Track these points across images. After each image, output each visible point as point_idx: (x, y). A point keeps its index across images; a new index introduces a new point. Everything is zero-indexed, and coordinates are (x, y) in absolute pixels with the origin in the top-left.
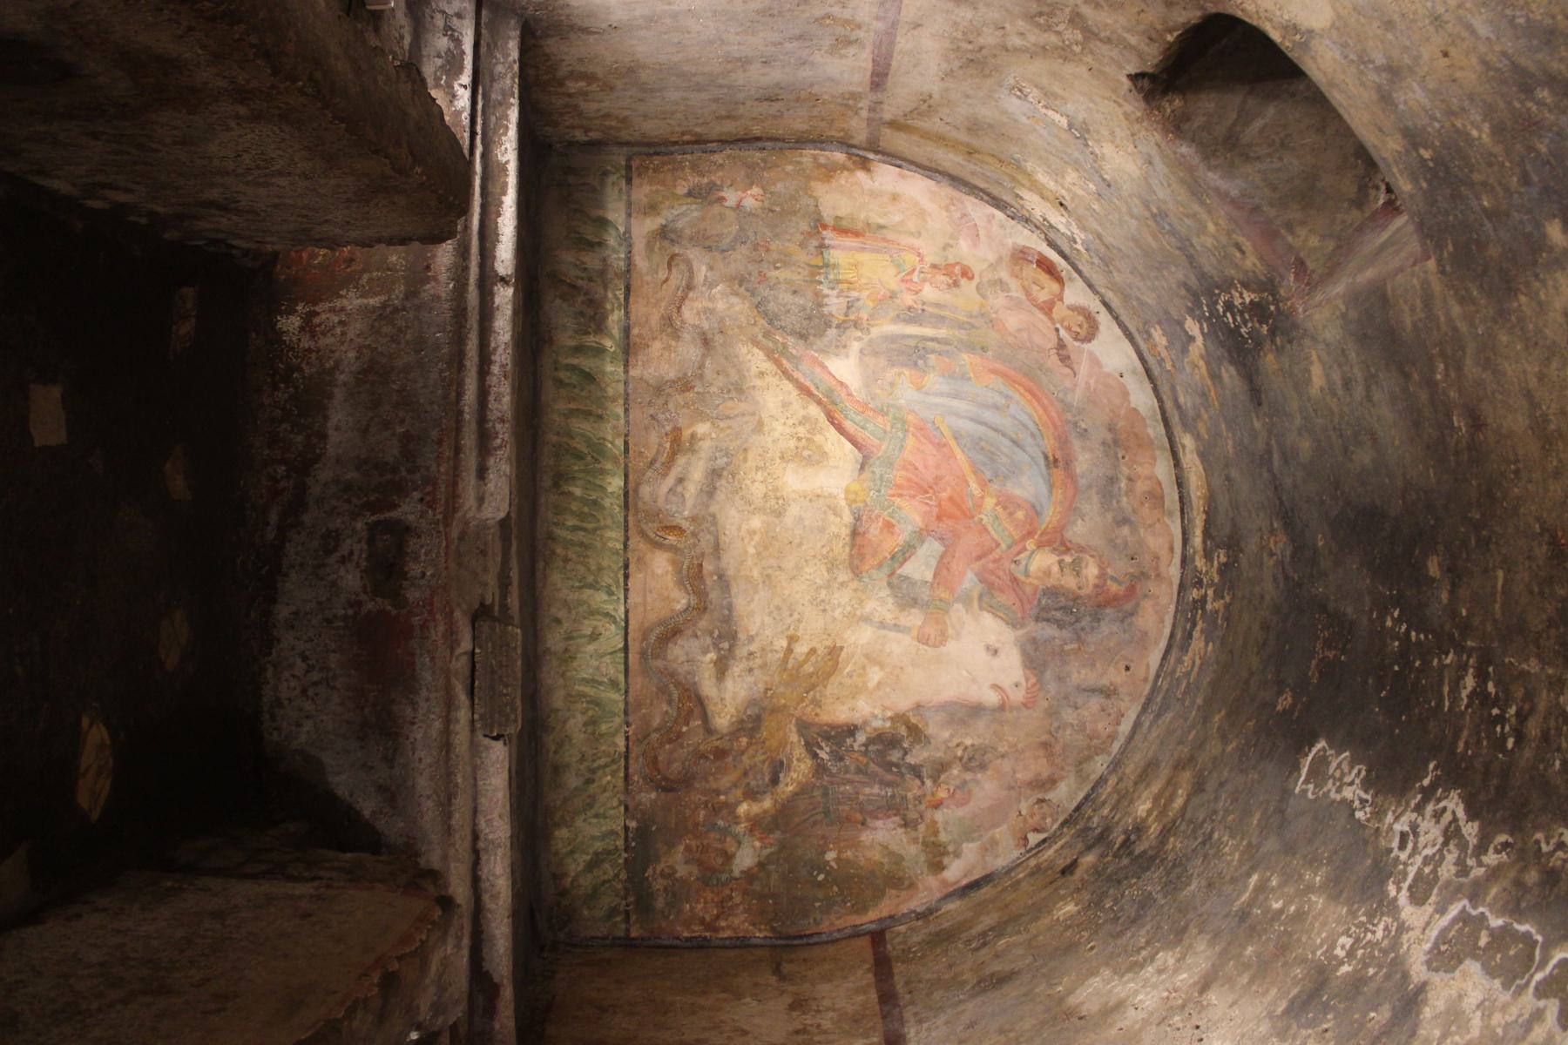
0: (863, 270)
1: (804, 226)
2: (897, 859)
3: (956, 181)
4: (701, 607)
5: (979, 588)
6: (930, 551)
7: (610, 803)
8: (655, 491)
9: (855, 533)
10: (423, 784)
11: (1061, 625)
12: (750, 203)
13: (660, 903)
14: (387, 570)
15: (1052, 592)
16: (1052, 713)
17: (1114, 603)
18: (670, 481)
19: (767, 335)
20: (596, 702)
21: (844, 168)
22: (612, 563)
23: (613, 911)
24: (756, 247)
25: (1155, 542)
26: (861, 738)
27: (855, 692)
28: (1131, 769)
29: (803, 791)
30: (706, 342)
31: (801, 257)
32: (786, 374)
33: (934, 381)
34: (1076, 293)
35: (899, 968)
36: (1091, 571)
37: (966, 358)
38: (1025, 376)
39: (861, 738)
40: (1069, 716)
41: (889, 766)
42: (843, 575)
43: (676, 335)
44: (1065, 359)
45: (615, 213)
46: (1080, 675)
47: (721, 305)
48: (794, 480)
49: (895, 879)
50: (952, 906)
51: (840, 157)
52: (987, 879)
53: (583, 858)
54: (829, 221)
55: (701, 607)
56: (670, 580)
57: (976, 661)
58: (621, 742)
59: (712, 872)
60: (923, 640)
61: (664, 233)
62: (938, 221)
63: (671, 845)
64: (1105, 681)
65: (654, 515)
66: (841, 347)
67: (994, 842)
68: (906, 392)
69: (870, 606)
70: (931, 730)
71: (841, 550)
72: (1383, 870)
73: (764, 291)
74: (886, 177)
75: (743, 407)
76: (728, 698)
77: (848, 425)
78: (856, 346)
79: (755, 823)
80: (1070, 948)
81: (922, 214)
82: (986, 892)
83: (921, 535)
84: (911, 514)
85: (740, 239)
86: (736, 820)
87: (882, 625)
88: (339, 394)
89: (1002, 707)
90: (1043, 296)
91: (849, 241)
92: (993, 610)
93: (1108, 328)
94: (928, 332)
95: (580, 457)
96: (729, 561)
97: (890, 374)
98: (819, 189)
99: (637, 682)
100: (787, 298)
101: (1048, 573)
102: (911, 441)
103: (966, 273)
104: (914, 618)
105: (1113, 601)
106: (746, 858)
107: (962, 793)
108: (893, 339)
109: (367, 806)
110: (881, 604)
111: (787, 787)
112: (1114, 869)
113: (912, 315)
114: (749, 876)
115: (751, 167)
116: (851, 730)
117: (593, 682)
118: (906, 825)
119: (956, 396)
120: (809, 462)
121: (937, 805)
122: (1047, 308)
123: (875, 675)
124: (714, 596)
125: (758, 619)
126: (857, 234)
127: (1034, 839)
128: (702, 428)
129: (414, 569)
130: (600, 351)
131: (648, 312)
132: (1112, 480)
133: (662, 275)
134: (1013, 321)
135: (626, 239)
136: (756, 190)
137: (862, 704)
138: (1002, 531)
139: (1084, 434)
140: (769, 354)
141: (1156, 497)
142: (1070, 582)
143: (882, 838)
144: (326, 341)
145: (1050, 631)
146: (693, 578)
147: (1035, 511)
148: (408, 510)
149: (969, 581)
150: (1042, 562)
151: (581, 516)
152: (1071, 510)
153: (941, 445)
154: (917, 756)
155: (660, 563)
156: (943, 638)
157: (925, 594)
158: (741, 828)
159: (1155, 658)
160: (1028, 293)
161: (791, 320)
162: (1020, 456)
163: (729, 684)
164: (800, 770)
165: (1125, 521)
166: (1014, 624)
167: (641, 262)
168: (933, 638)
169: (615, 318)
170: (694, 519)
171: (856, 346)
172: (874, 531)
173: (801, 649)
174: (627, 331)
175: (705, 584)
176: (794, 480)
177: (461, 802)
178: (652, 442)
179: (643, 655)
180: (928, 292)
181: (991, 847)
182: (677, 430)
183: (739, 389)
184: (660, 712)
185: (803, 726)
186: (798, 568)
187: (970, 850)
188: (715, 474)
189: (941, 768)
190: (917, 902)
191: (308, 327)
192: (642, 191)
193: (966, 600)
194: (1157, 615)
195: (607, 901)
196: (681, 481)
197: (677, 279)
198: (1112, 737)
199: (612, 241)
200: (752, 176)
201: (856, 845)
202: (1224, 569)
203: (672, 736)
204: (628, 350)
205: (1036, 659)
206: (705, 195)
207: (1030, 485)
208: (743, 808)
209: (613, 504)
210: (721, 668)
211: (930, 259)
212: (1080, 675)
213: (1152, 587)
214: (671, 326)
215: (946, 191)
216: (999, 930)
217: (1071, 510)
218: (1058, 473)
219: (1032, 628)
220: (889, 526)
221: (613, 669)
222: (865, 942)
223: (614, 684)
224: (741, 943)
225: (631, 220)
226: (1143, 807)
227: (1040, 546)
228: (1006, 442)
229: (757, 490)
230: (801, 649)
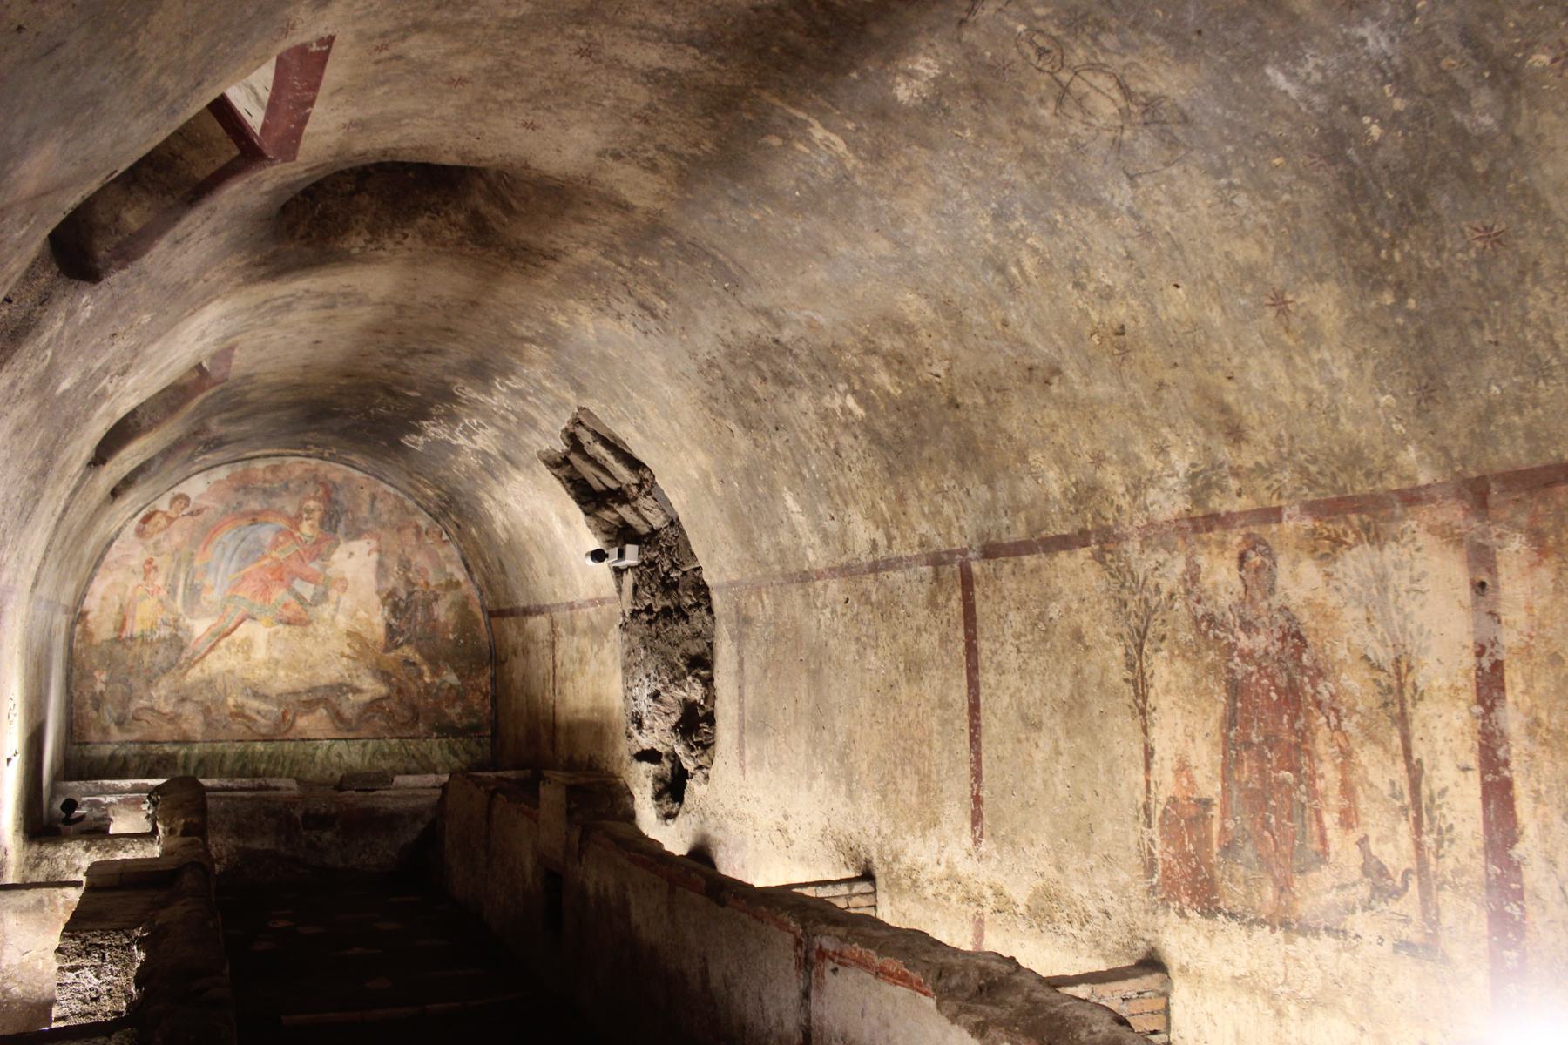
0: (144, 617)
1: (118, 647)
2: (453, 604)
3: (97, 565)
4: (325, 701)
5: (318, 561)
6: (298, 585)
7: (424, 746)
8: (264, 725)
9: (289, 623)
10: (411, 804)
11: (338, 521)
12: (104, 677)
13: (475, 721)
14: (321, 821)
15: (322, 524)
16: (383, 526)
17: (329, 493)
18: (259, 718)
19: (180, 667)
20: (374, 754)
21: (85, 626)
22: (302, 747)
23: (479, 744)
24: (130, 674)
25: (298, 471)
26: (393, 621)
27: (370, 623)
28: (412, 491)
29: (419, 650)
30: (183, 700)
31: (137, 649)
32: (203, 657)
33: (209, 581)
34: (163, 504)
35: (502, 606)
36: (312, 504)
37: (197, 563)
38: (208, 533)
39: (393, 621)
40: (385, 517)
41: (407, 608)
42: (310, 629)
43: (179, 716)
44: (199, 512)
45: (107, 750)
46: (364, 512)
47: (163, 692)
48: (260, 654)
49: (463, 606)
50: (476, 577)
51: (78, 628)
52: (464, 560)
53: (453, 759)
54: (115, 635)
55: (325, 701)
56: (311, 717)
57: (356, 564)
58: (394, 741)
59: (459, 695)
60: (344, 589)
61: (120, 723)
62: (119, 576)
63: (446, 715)
64: (368, 500)
65: (277, 726)
66: (188, 629)
67: (446, 556)
68: (214, 595)
69: (326, 616)
70: (390, 586)
71: (297, 630)
72: (448, 442)
73: (156, 669)
74: (91, 603)
75: (220, 680)
76: (371, 687)
77: (231, 625)
78: (188, 621)
79: (435, 673)
80: (487, 535)
81: (114, 584)
82: (470, 562)
83: (290, 589)
84: (279, 594)
85: (125, 682)
86: (433, 683)
87: (336, 610)
88: (248, 845)
89: (380, 551)
90: (164, 522)
91: (129, 624)
92: (329, 555)
93: (183, 489)
94: (181, 583)
95: (244, 765)
96: (301, 687)
97: (204, 603)
98: (97, 639)
99: (363, 733)
100: (159, 658)
101: (312, 526)
102: (241, 594)
103: (149, 562)
104: (333, 594)
105: (327, 493)
106: (452, 678)
107: (421, 571)
108: (184, 601)
109: (420, 826)
110: (325, 611)
111: (417, 658)
112: (455, 511)
113: (172, 591)
114: (460, 677)
115: (82, 676)
116: (389, 626)
117: (363, 755)
118: (436, 600)
119: (217, 569)
120: (250, 646)
121: (427, 584)
122: (170, 520)
123: (362, 614)
124: (319, 695)
125: (332, 672)
126: (125, 620)
127: (445, 537)
128: (231, 701)
129: (323, 810)
130: (187, 756)
131: (165, 731)
132: (265, 491)
133: (144, 724)
134: (177, 538)
135: (122, 744)
136: (96, 674)
137: (376, 621)
138: (290, 548)
139: (240, 504)
140: (191, 666)
141: (275, 469)
142: (317, 515)
143: (443, 612)
144: (224, 852)
145: (342, 526)
146: (310, 706)
147: (280, 531)
148: (298, 813)
149: (315, 566)
150: (306, 528)
151: (277, 764)
152: (280, 513)
153: (244, 578)
154: (403, 594)
155: (302, 722)
156: (343, 580)
157: (321, 588)
158: (437, 681)
159: (357, 474)
160: (161, 530)
161: (173, 655)
162: (251, 537)
163: (365, 687)
164: (408, 651)
165: (286, 487)
166: (337, 544)
167: (137, 735)
168: (344, 584)
169: (168, 749)
170: (279, 706)
171: (188, 621)
172: (288, 613)
173: (348, 651)
174: (175, 742)
175: (312, 699)
176: (260, 654)
177: (420, 792)
178: (238, 727)
179: (349, 731)
180: (160, 582)
181: (449, 558)
182: (231, 714)
183: (210, 683)
184: (379, 722)
185: (387, 650)
186: (306, 652)
187: (449, 568)
188: (256, 695)
189: (409, 582)
190: (475, 595)
191: (218, 860)
192: (94, 736)
193: (325, 567)
194: (336, 472)
195: (473, 746)
196: (259, 713)
197: (147, 716)
198: (396, 497)
199: (123, 752)
200: (88, 676)
201: (446, 624)
202: (316, 445)
203: (390, 715)
204: (186, 741)
205: (355, 533)
206: (98, 702)
207: (266, 533)
208: (427, 680)
209: (271, 747)
210: (357, 691)
211: (140, 581)
212: (364, 512)
213: (321, 473)
214: (173, 719)
215: (101, 571)
216: (484, 561)
217: (280, 513)
218: (260, 518)
219: (340, 535)
220: (286, 606)
221: (357, 746)
222: (493, 620)
223: (364, 745)
224: (494, 680)
225: (114, 741)
226: (429, 492)
227: (298, 529)
228: (244, 545)
229: (265, 673)
230: (348, 651)
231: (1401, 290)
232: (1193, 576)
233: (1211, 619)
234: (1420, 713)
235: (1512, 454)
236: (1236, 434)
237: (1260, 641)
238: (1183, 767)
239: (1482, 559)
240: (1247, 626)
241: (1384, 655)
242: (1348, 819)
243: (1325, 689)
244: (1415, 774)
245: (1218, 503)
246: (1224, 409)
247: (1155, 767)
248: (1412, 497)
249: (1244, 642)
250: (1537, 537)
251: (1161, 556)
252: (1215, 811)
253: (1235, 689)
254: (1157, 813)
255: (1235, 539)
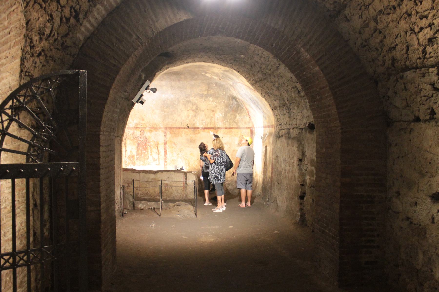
231: (165, 112)
232: (134, 133)
233: (136, 137)
234: (159, 146)
235: (169, 126)
236: (143, 120)
237: (142, 139)
238: (131, 152)
239: (165, 133)
240: (140, 138)
241: (156, 141)
242: (151, 155)
243: (149, 144)
244: (158, 151)
245: (138, 126)
246: (143, 118)
247: (127, 152)
248: (160, 128)
249: (140, 139)
250: (170, 132)
251: (129, 130)
252: (135, 156)
253: (138, 144)
254: (127, 157)
255: (140, 130)
